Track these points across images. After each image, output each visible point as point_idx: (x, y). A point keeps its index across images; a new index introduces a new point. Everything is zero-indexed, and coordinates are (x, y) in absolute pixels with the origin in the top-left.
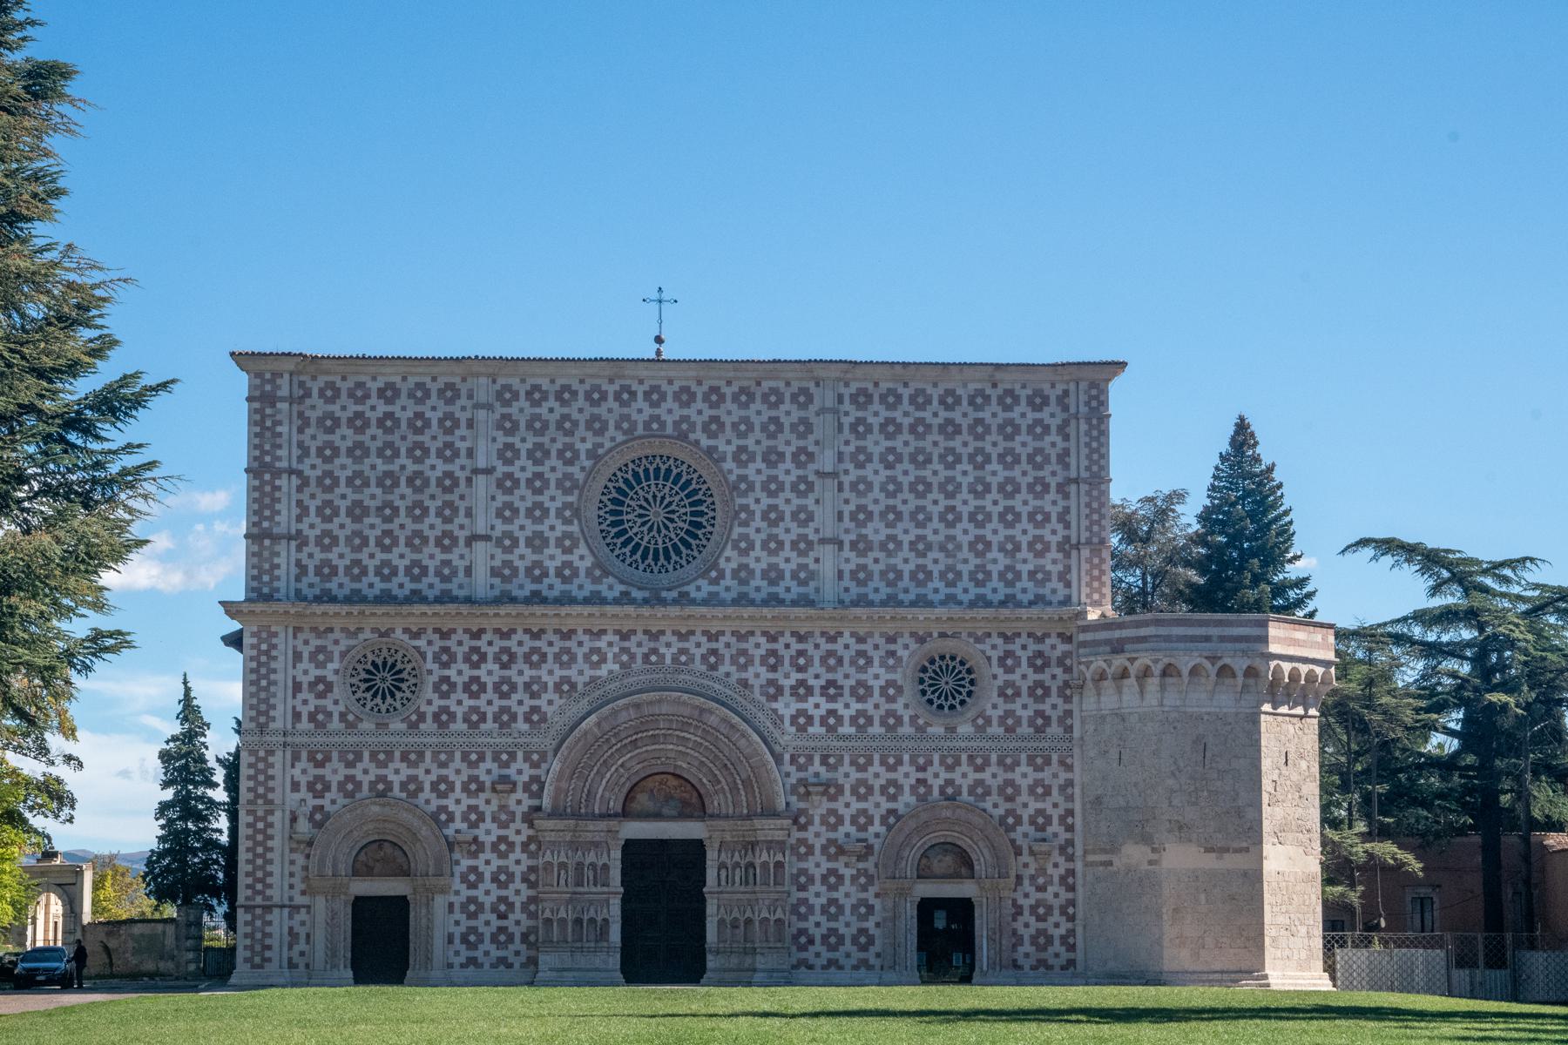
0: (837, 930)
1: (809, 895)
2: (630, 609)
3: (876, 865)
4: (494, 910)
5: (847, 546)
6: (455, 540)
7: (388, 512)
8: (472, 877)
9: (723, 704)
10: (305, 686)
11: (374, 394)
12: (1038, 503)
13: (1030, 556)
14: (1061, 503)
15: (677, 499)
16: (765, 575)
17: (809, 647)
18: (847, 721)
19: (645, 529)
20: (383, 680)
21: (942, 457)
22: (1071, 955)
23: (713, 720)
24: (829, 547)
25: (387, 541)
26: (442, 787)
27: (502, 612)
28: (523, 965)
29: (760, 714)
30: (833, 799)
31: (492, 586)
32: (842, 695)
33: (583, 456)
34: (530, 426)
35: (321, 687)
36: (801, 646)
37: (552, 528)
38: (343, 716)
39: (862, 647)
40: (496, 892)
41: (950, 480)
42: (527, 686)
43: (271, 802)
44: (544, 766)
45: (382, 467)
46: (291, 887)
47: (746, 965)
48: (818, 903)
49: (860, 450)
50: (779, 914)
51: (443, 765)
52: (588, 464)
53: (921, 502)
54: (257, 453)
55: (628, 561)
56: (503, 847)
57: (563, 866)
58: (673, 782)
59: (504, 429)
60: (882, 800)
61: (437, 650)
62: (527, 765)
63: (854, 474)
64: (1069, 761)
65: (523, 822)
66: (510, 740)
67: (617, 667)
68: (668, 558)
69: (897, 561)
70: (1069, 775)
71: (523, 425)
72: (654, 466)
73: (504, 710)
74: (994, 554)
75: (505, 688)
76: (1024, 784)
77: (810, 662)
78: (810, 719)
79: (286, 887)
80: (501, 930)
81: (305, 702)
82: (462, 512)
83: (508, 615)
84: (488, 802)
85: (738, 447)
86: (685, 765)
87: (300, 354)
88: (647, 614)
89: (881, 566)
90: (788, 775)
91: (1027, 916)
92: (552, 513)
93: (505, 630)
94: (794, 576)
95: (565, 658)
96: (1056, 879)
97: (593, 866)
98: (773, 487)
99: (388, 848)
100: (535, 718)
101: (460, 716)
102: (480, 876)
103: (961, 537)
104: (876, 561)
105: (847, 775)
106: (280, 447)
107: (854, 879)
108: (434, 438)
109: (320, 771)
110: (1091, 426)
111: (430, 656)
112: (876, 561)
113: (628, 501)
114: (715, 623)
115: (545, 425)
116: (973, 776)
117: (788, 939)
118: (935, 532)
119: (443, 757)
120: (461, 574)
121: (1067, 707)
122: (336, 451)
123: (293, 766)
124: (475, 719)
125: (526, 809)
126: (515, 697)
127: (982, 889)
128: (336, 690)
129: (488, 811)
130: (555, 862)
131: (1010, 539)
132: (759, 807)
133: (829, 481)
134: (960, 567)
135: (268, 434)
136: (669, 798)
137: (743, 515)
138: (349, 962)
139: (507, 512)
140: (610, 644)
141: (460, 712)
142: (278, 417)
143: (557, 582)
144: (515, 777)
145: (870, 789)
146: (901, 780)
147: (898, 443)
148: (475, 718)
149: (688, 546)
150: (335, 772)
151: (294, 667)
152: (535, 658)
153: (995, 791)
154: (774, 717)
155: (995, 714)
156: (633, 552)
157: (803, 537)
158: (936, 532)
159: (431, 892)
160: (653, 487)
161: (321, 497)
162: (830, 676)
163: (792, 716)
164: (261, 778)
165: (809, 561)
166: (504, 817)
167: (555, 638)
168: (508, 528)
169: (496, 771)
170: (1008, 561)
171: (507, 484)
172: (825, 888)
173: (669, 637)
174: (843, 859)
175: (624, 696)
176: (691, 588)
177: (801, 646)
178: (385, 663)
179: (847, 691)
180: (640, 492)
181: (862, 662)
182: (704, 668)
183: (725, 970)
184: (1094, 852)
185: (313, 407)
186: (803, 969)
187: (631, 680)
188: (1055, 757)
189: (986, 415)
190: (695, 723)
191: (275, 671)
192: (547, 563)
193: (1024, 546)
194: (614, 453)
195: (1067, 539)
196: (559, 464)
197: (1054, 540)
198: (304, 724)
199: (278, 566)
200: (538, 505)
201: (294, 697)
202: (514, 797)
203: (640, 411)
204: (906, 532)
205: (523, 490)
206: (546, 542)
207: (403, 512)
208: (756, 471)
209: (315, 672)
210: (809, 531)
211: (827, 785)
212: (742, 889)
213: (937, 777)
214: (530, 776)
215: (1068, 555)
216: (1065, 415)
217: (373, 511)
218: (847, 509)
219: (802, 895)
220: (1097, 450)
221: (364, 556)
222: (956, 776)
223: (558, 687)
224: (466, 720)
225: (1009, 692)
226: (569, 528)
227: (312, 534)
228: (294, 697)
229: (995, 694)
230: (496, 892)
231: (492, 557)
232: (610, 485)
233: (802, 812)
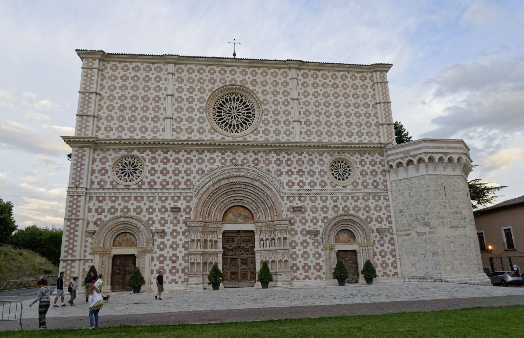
0: (307, 264)
1: (296, 250)
3: (322, 238)
4: (171, 259)
6: (159, 119)
7: (134, 108)
8: (162, 246)
9: (261, 177)
10: (97, 171)
11: (131, 69)
12: (367, 110)
13: (366, 127)
14: (374, 111)
18: (307, 184)
20: (129, 169)
21: (333, 95)
22: (396, 271)
23: (257, 184)
24: (297, 123)
25: (133, 119)
26: (150, 210)
28: (182, 282)
31: (172, 135)
33: (207, 91)
34: (188, 81)
35: (103, 172)
36: (289, 157)
38: (111, 183)
39: (311, 157)
40: (172, 252)
41: (336, 102)
42: (185, 171)
43: (78, 216)
45: (132, 93)
46: (85, 251)
48: (300, 253)
49: (305, 92)
50: (286, 258)
51: (151, 202)
53: (327, 109)
54: (84, 86)
57: (199, 240)
58: (241, 209)
59: (179, 81)
60: (322, 213)
61: (150, 158)
63: (304, 99)
64: (387, 198)
66: (179, 191)
67: (220, 165)
68: (238, 128)
69: (321, 128)
70: (388, 203)
71: (185, 80)
73: (176, 180)
74: (354, 126)
75: (177, 172)
76: (372, 206)
77: (292, 162)
78: (293, 183)
79: (83, 251)
80: (174, 268)
81: (96, 177)
82: (162, 109)
86: (246, 202)
87: (102, 51)
89: (315, 130)
91: (378, 256)
92: (196, 110)
96: (387, 242)
97: (211, 241)
98: (276, 103)
99: (128, 236)
100: (188, 183)
101: (158, 183)
102: (165, 246)
103: (342, 121)
104: (313, 128)
105: (308, 204)
106: (93, 84)
107: (313, 243)
108: (152, 84)
109: (101, 204)
110: (382, 86)
111: (147, 160)
112: (313, 128)
113: (223, 108)
115: (194, 81)
116: (354, 204)
118: (333, 119)
119: (151, 198)
120: (161, 130)
121: (385, 179)
122: (115, 88)
123: (89, 202)
124: (165, 184)
126: (180, 175)
127: (359, 246)
128: (109, 173)
129: (169, 219)
130: (196, 240)
131: (359, 122)
133: (296, 101)
134: (342, 131)
135: (89, 80)
136: (240, 215)
138: (109, 283)
139: (179, 110)
140: (218, 156)
141: (158, 181)
142: (93, 74)
145: (317, 209)
146: (328, 206)
147: (318, 90)
150: (107, 204)
151: (93, 164)
152: (189, 161)
153: (362, 209)
155: (360, 181)
156: (226, 126)
158: (333, 119)
159: (144, 252)
161: (108, 103)
162: (300, 168)
164: (75, 206)
165: (290, 128)
168: (179, 115)
170: (359, 129)
171: (180, 99)
176: (247, 137)
177: (289, 157)
178: (130, 163)
179: (306, 173)
181: (311, 163)
182: (253, 165)
184: (401, 231)
185: (108, 73)
186: (295, 280)
188: (382, 197)
189: (347, 82)
191: (84, 165)
193: (364, 124)
195: (377, 122)
196: (198, 93)
197: (373, 123)
198: (96, 186)
199: (89, 126)
201: (92, 175)
203: (228, 77)
204: (323, 119)
205: (185, 102)
207: (139, 109)
208: (269, 97)
209: (101, 166)
210: (289, 118)
213: (341, 204)
215: (378, 127)
216: (373, 83)
217: (128, 108)
218: (302, 111)
219: (294, 250)
220: (385, 93)
221: (123, 124)
222: (348, 203)
223: (197, 172)
224: (161, 184)
225: (364, 173)
226: (202, 115)
227: (104, 116)
228: (92, 175)
229: (359, 174)
230: (172, 252)
231: (173, 125)
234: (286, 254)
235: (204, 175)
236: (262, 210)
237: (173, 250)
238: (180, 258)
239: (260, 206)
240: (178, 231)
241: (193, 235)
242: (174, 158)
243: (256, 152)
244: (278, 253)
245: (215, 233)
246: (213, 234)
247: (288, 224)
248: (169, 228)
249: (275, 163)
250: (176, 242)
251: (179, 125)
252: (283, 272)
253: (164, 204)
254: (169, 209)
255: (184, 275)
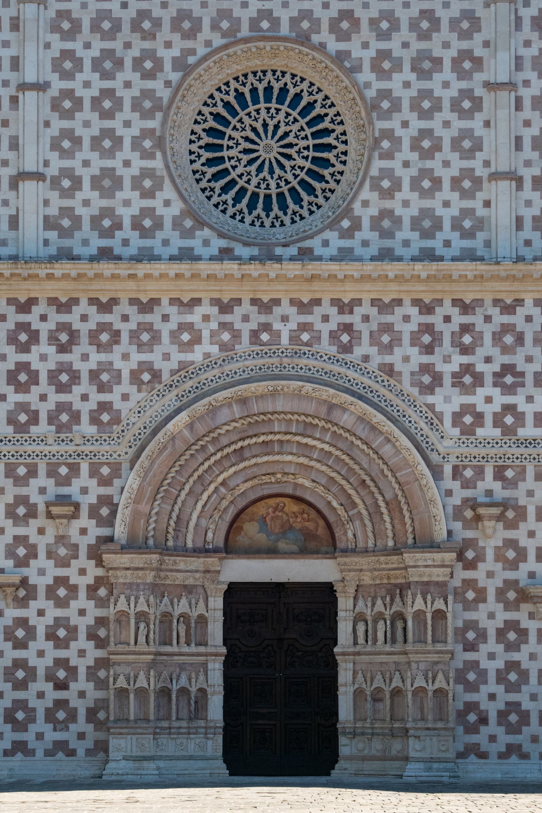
0: (519, 704)
2: (231, 267)
4: (50, 677)
5: (528, 184)
8: (20, 633)
9: (361, 397)
15: (295, 128)
16: (415, 224)
17: (477, 319)
19: (253, 168)
23: (346, 420)
24: (504, 185)
27: (58, 273)
28: (89, 752)
29: (410, 411)
30: (511, 525)
31: (46, 242)
32: (523, 385)
33: (168, 66)
34: (95, 27)
36: (467, 319)
37: (127, 164)
42: (94, 375)
44: (117, 482)
47: (394, 752)
50: (441, 682)
52: (175, 77)
55: (231, 211)
56: (62, 592)
57: (141, 616)
58: (292, 507)
62: (95, 481)
65: (89, 558)
66: (71, 448)
67: (215, 349)
68: (284, 207)
71: (86, 25)
72: (265, 84)
73: (61, 407)
75: (64, 378)
77: (478, 339)
78: (479, 417)
80: (60, 704)
83: (65, 277)
84: (41, 531)
85: (378, 51)
86: (307, 483)
88: (255, 274)
90: (449, 493)
92: (127, 143)
93: (64, 300)
94: (456, 225)
95: (145, 337)
98: (426, 104)
100: (105, 417)
102: (31, 632)
113: (229, 131)
114: (348, 286)
115: (117, 26)
117: (452, 717)
125: (93, 541)
126: (77, 390)
130: (132, 612)
132: (410, 537)
133: (503, 95)
137: (386, 144)
140: (206, 318)
143: (134, 236)
144: (77, 497)
148: (23, 418)
149: (311, 190)
152: (104, 337)
154: (430, 415)
156: (237, 199)
157: (468, 173)
160: (263, 112)
162: (507, 359)
163: (454, 414)
165: (477, 204)
166: (62, 551)
167: (132, 311)
168: (67, 163)
169: (52, 490)
172: (501, 647)
173: (286, 308)
174: (526, 608)
175: (225, 388)
176: (315, 243)
177: (467, 319)
180: (246, 119)
182: (333, 350)
183: (364, 759)
186: (472, 758)
187: (234, 366)
190: (322, 424)
192: (121, 211)
194: (209, 62)
196: (135, 77)
200: (108, 133)
202: (76, 525)
206: (118, 183)
211: (504, 505)
212: (388, 648)
214: (99, 497)
219: (470, 656)
223: (135, 377)
226: (148, 164)
231: (46, 203)
232: (206, 110)
233: (469, 543)
234: (440, 666)
235: (158, 387)
236: (364, 512)
237: (56, 647)
238: (82, 672)
239: (358, 501)
240: (72, 582)
241: (122, 597)
242: (54, 327)
243: (346, 301)
244: (414, 666)
245: (200, 590)
246: (190, 593)
247: (451, 566)
248: (42, 572)
249: (415, 340)
250: (68, 619)
251: (67, 203)
252: (428, 729)
253: (23, 491)
254: (41, 508)
255: (96, 730)
